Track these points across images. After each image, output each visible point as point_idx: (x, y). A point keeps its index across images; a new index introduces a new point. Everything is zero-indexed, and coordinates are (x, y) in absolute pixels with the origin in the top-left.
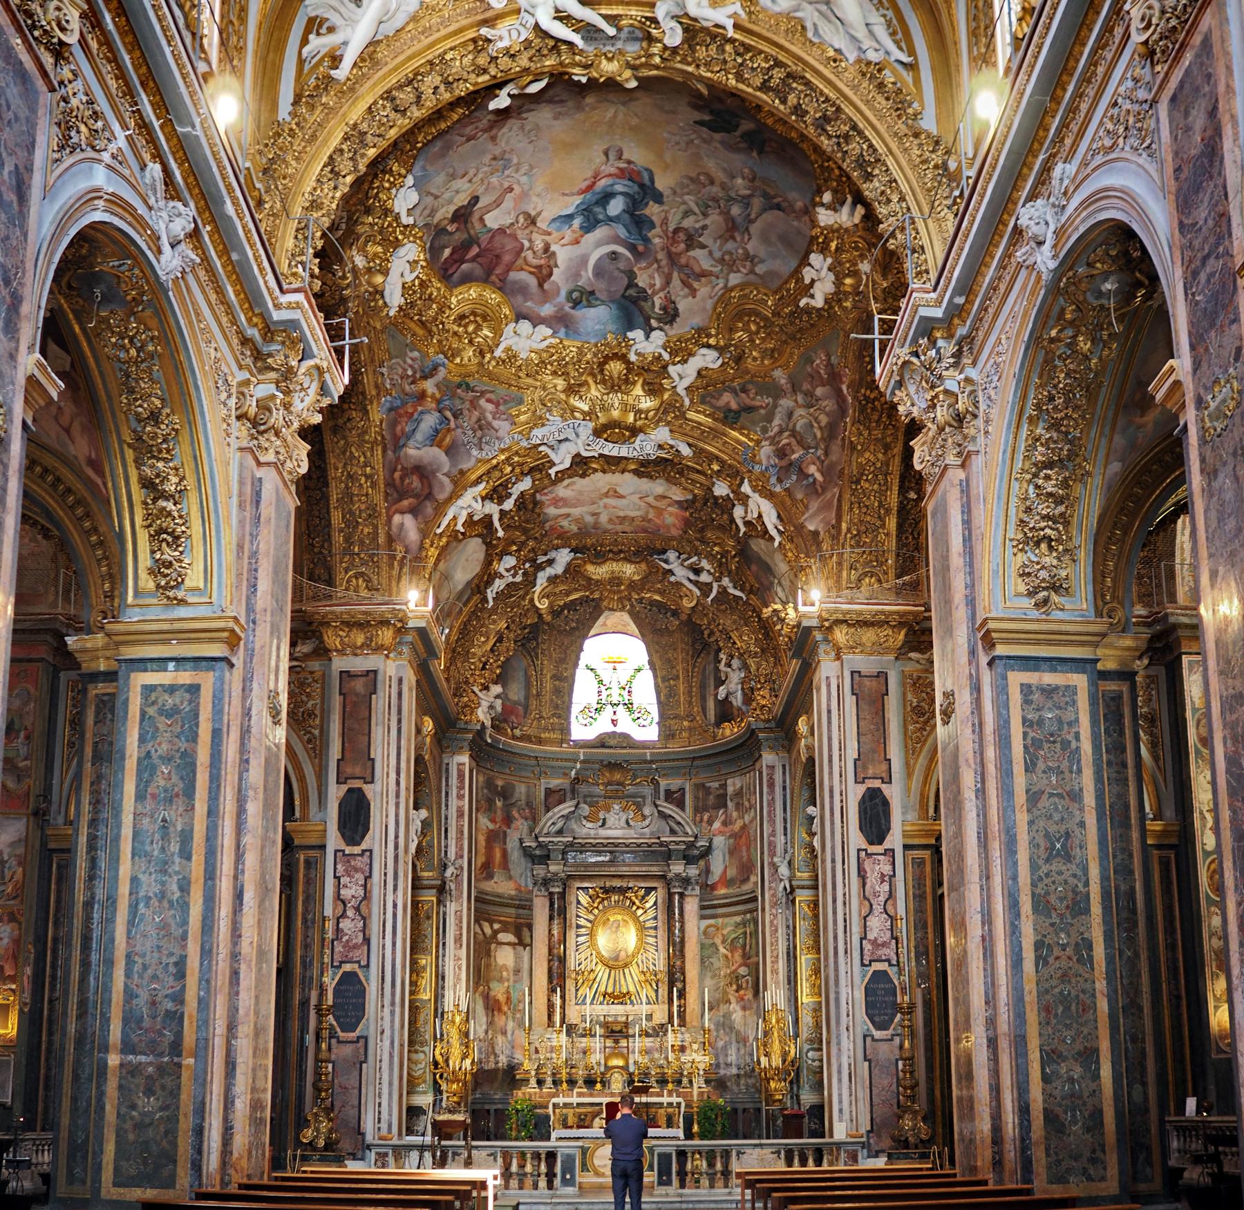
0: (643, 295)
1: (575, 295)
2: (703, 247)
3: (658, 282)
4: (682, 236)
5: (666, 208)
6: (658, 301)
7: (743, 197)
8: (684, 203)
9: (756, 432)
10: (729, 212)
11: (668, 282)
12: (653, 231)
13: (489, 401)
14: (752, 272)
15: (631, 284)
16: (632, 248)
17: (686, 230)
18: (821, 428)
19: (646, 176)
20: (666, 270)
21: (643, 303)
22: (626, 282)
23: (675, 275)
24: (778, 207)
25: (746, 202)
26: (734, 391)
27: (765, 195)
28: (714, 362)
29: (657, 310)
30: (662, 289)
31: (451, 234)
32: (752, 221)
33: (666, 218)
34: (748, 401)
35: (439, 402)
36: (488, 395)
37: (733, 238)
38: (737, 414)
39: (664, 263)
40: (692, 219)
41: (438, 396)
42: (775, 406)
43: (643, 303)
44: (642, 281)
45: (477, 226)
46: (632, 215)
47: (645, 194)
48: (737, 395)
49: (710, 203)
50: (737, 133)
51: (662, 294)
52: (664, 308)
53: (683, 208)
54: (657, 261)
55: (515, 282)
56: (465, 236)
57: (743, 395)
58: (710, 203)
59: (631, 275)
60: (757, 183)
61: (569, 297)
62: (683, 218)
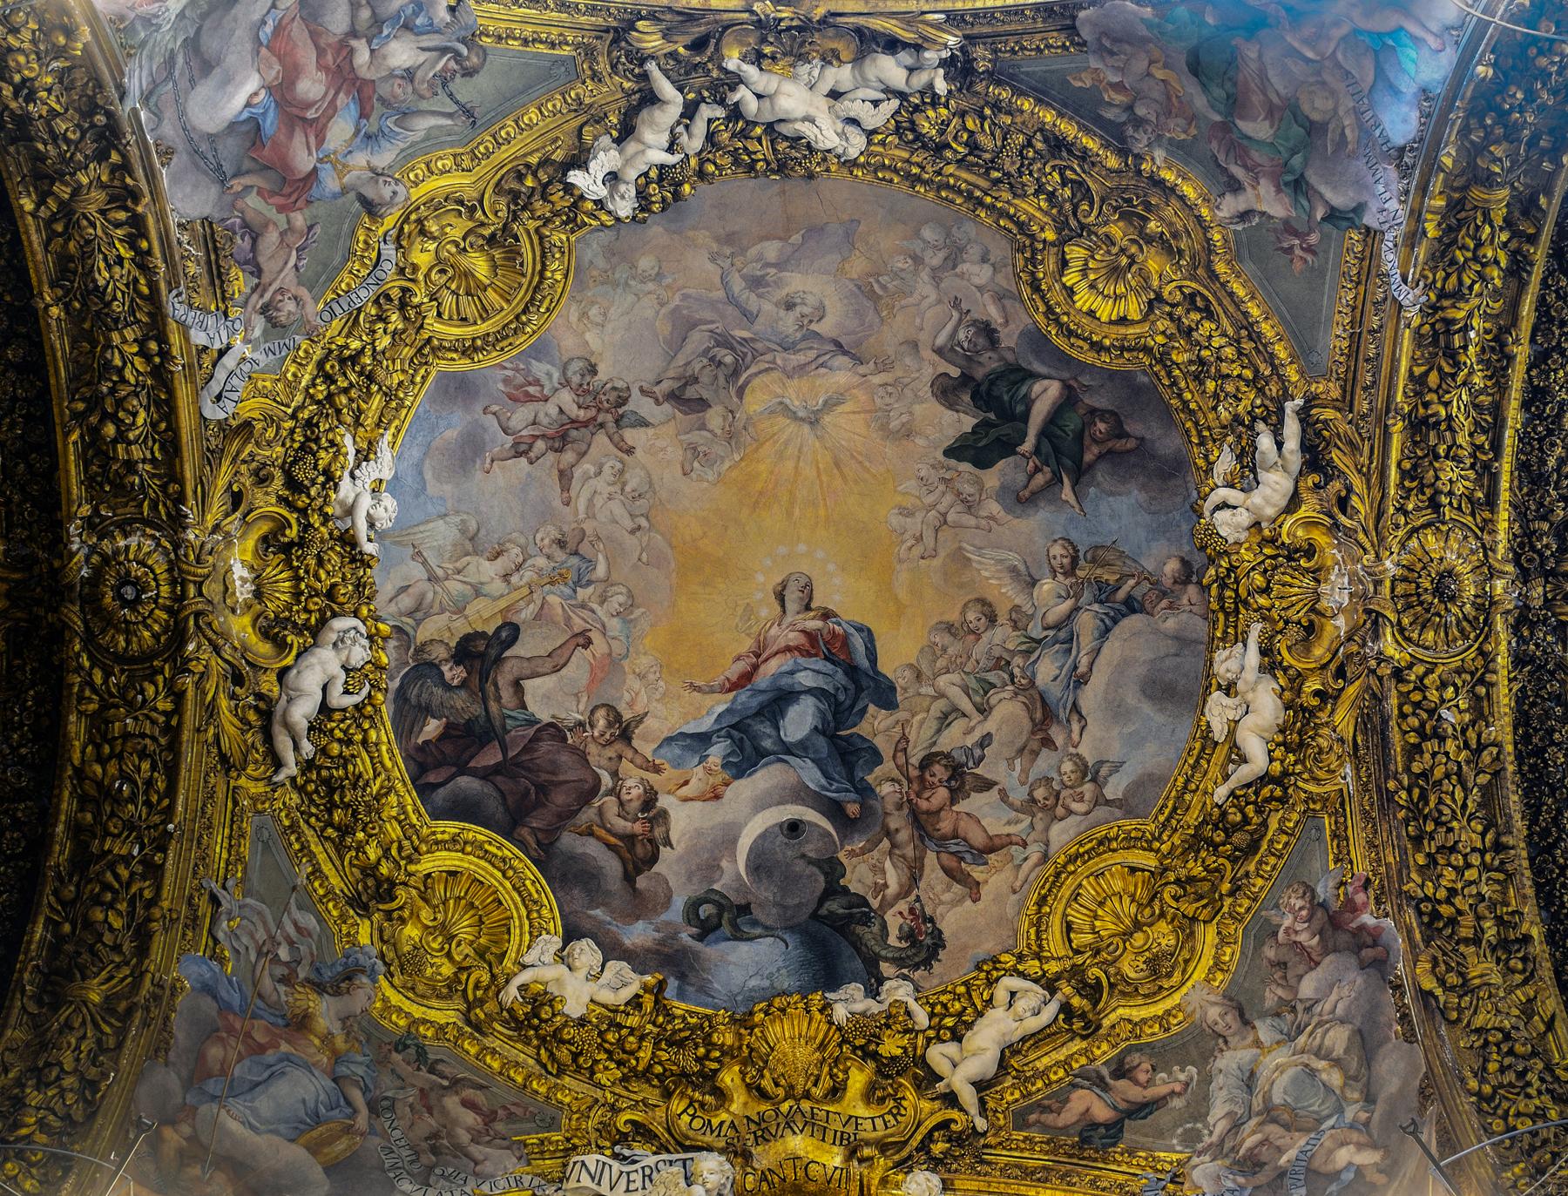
0: (860, 912)
5: (901, 715)
8: (942, 695)
9: (1171, 1150)
12: (878, 770)
19: (858, 642)
26: (1099, 1083)
28: (1036, 1013)
33: (904, 738)
34: (1136, 1094)
38: (1114, 1130)
40: (958, 726)
47: (859, 689)
53: (941, 705)
54: (888, 834)
62: (939, 731)
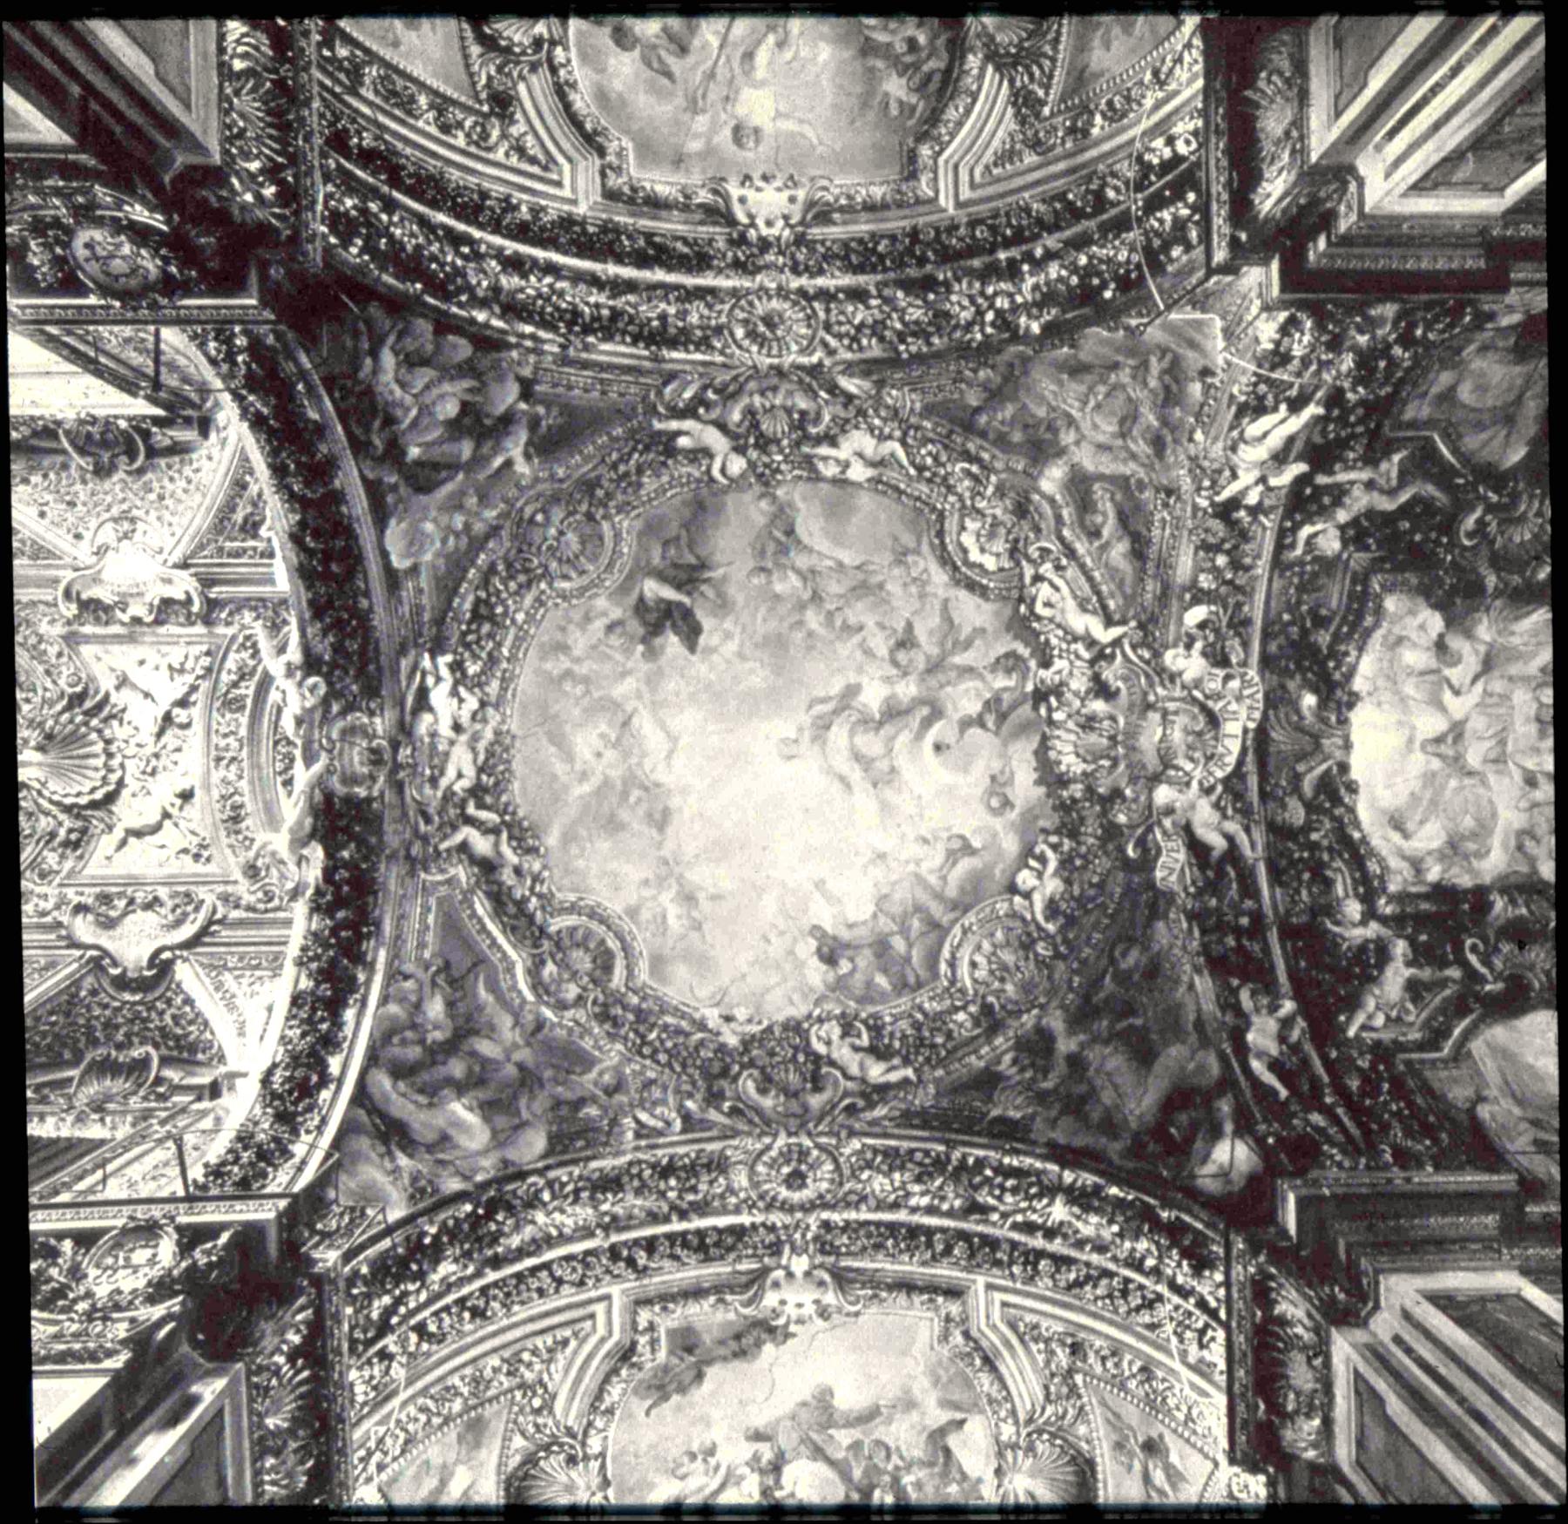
1: (995, 803)
2: (909, 627)
3: (971, 684)
4: (902, 656)
6: (1001, 682)
7: (805, 579)
10: (841, 596)
11: (968, 671)
13: (1124, 955)
14: (917, 552)
15: (980, 722)
16: (927, 723)
17: (892, 652)
18: (1091, 389)
20: (953, 674)
21: (1005, 705)
22: (975, 731)
23: (958, 659)
24: (790, 532)
25: (808, 575)
27: (783, 550)
29: (1012, 683)
30: (983, 678)
31: (854, 970)
32: (840, 564)
35: (1095, 1039)
36: (1117, 953)
37: (881, 586)
39: (942, 677)
41: (1082, 1037)
42: (1101, 477)
43: (1005, 705)
44: (973, 707)
45: (857, 932)
46: (881, 724)
48: (1108, 544)
49: (838, 623)
50: (686, 600)
51: (989, 677)
52: (1009, 671)
55: (962, 890)
56: (867, 952)
57: (1106, 532)
58: (838, 623)
59: (966, 724)
60: (770, 565)
61: (995, 812)
